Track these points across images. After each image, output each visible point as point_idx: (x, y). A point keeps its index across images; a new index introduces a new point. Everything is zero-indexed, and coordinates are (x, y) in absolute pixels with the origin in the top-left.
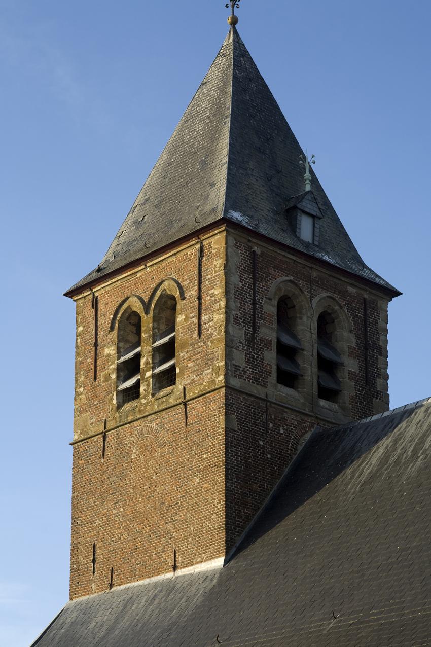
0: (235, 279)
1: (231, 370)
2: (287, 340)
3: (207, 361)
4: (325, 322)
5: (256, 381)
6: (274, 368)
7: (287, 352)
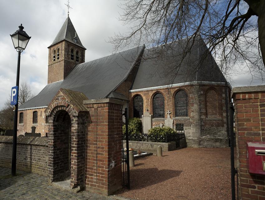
0: (66, 47)
1: (65, 58)
2: (72, 54)
3: (62, 56)
4: (77, 53)
5: (68, 59)
7: (72, 56)
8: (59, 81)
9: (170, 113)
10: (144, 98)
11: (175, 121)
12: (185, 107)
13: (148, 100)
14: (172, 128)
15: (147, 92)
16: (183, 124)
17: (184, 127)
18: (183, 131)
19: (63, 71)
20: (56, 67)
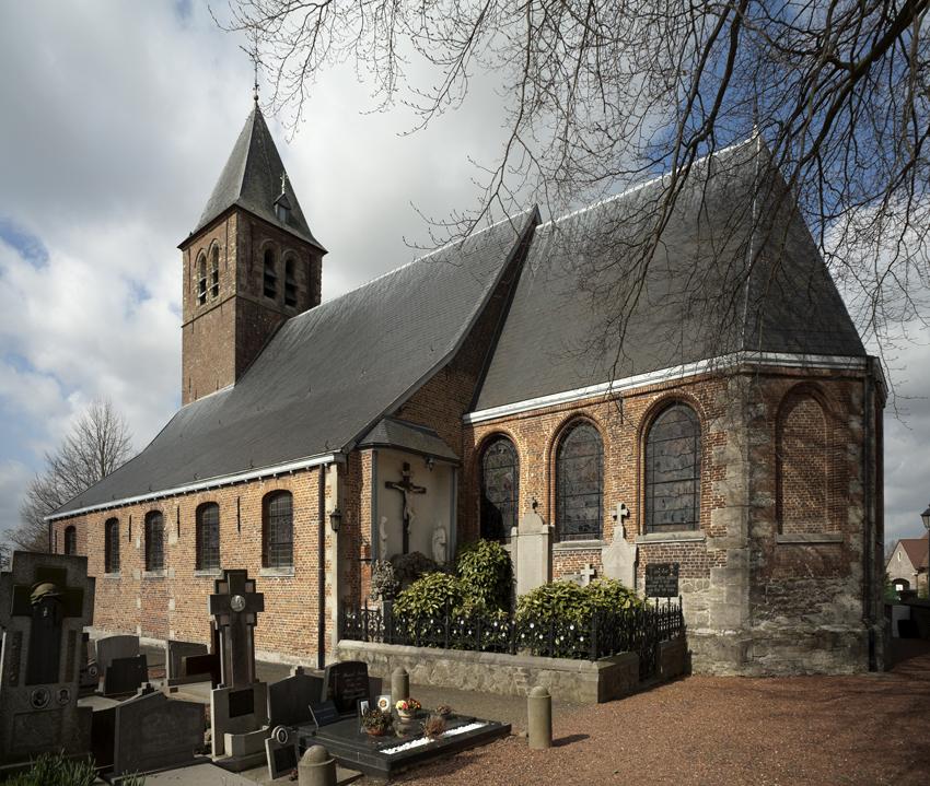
0: (241, 238)
1: (239, 287)
2: (269, 273)
5: (253, 293)
6: (262, 287)
7: (270, 280)
8: (219, 391)
9: (623, 517)
10: (522, 447)
11: (643, 553)
12: (689, 484)
13: (539, 456)
14: (628, 584)
15: (533, 421)
16: (677, 566)
17: (680, 581)
18: (674, 600)
19: (234, 348)
20: (208, 329)
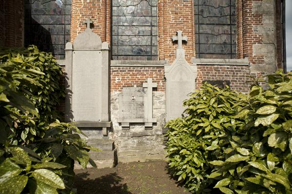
12: (226, 27)
